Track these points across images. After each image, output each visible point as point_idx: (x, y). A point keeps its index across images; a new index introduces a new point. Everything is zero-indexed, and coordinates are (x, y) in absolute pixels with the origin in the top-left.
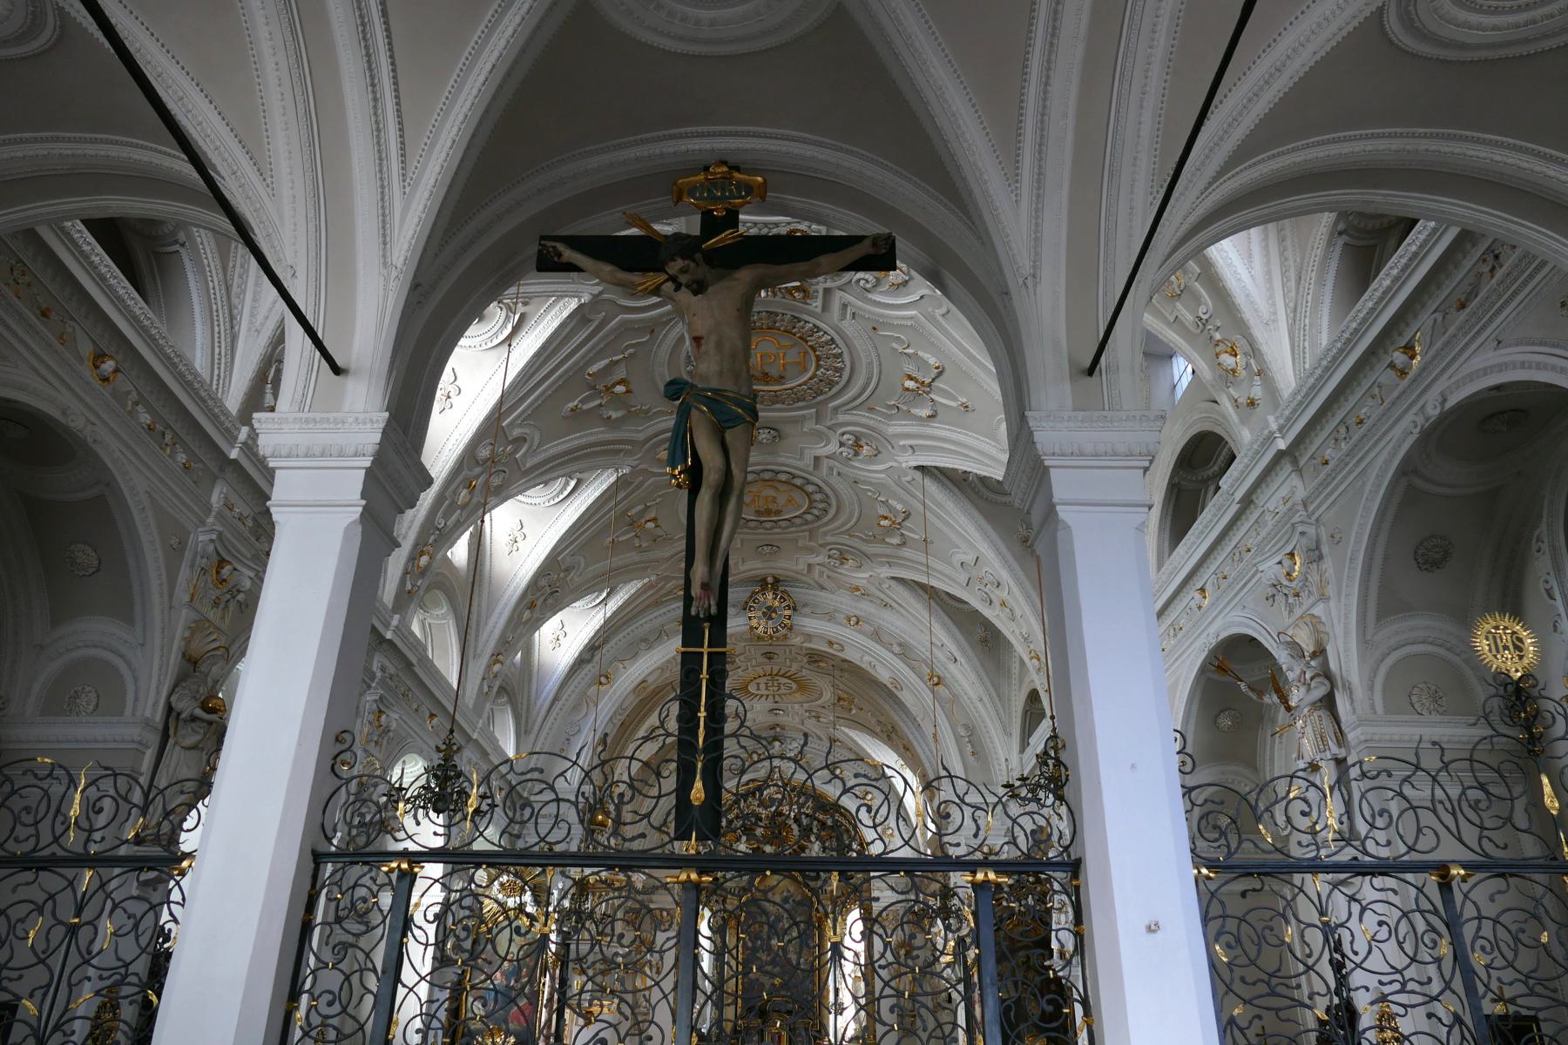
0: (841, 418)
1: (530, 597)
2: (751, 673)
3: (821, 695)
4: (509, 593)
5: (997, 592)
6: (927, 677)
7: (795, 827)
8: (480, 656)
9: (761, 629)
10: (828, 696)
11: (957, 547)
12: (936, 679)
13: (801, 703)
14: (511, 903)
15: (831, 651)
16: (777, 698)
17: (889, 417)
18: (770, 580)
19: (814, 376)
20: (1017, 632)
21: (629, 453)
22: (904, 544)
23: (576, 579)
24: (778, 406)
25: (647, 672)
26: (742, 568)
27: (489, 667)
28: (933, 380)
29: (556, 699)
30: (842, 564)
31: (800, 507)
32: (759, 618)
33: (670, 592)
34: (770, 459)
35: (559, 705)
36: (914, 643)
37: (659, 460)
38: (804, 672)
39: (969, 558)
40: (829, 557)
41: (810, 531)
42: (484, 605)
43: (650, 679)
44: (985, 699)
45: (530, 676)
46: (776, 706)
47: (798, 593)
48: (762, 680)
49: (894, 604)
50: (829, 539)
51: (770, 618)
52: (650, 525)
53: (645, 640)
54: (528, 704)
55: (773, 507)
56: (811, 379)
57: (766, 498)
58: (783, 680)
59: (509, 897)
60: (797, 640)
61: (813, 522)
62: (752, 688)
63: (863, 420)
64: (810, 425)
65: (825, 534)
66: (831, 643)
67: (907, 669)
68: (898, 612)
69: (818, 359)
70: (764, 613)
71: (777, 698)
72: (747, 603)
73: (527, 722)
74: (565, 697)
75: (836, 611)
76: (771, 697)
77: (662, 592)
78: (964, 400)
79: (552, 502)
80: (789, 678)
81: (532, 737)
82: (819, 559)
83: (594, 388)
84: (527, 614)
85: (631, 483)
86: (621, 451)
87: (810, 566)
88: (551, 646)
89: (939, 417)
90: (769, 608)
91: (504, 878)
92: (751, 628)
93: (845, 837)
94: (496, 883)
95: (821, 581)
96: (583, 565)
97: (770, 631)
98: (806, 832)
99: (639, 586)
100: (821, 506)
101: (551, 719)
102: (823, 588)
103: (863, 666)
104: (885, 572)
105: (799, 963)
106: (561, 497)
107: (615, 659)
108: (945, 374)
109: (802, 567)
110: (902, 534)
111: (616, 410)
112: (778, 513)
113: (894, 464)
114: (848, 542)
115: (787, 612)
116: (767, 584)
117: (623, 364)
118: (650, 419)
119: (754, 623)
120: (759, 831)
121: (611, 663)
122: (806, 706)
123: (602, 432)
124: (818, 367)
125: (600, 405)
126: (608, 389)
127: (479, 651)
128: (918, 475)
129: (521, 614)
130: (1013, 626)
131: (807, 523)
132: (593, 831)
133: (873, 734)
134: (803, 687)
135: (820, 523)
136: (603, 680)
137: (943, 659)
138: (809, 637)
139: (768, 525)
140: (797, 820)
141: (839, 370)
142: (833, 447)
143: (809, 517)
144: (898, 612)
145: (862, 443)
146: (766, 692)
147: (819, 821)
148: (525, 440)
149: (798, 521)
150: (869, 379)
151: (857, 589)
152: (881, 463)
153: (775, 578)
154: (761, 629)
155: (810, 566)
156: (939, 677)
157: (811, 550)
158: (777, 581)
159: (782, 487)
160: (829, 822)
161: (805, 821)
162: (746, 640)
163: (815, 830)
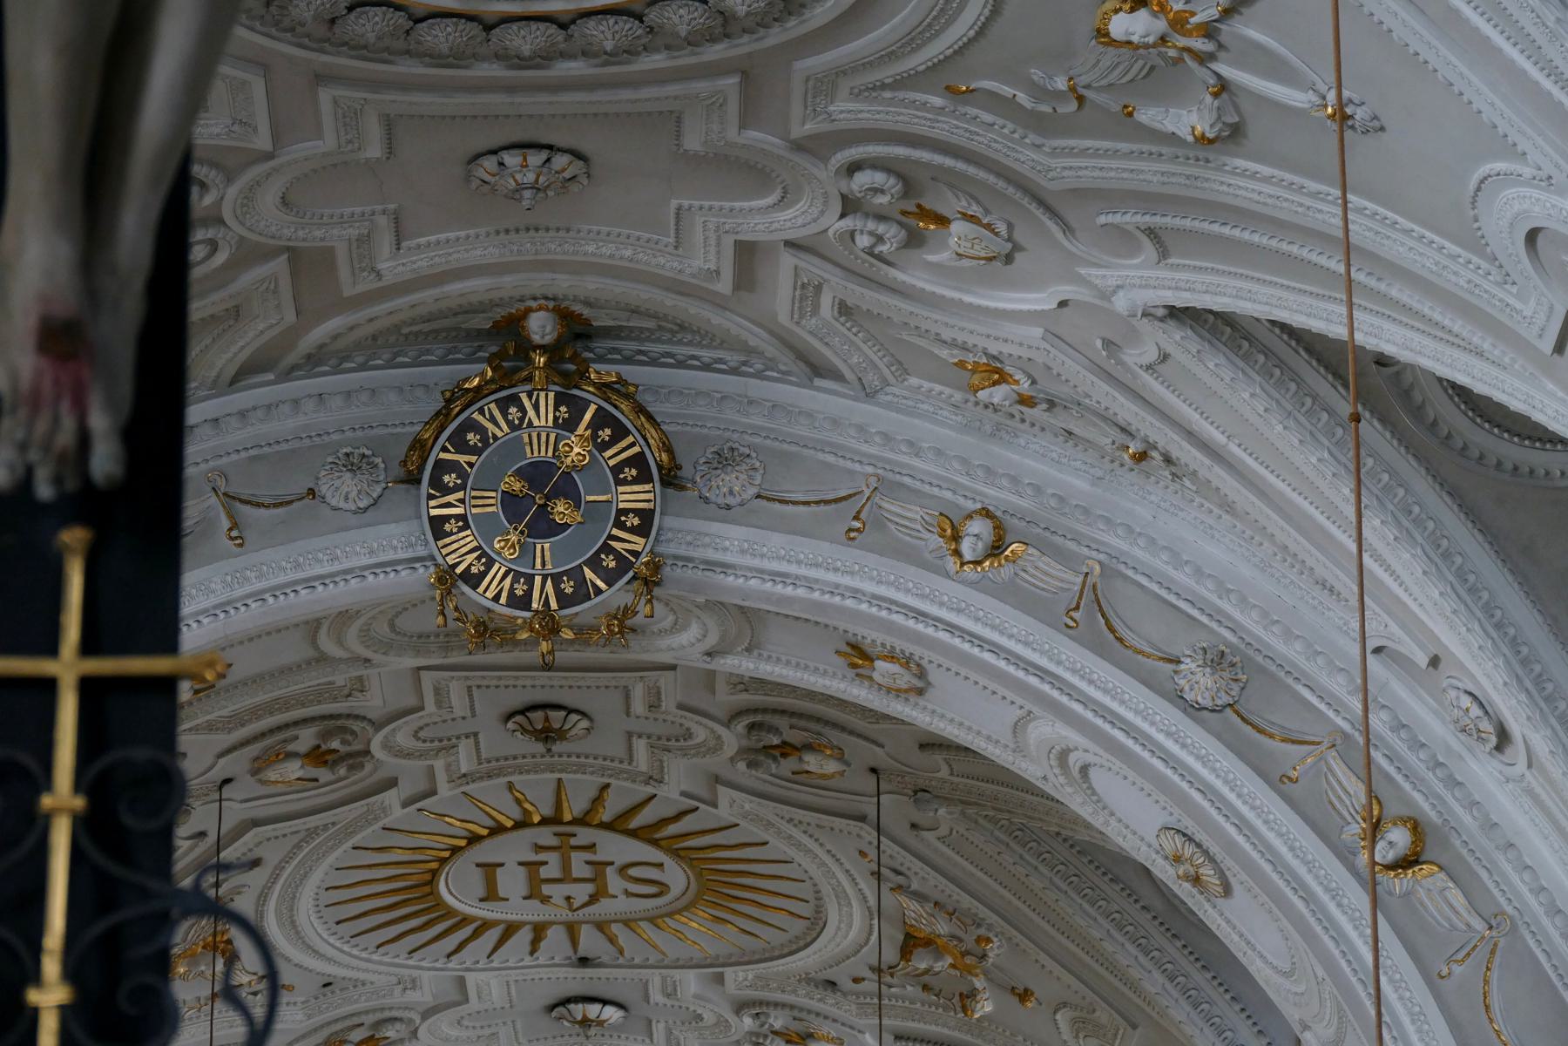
3: (816, 924)
6: (1356, 828)
9: (495, 582)
11: (1512, 152)
12: (1397, 839)
13: (714, 968)
15: (859, 693)
16: (590, 941)
18: (541, 327)
22: (1232, 135)
26: (391, 267)
30: (914, 240)
32: (488, 527)
36: (1293, 652)
38: (730, 805)
40: (849, 206)
41: (747, 74)
48: (512, 851)
50: (846, 110)
51: (544, 526)
65: (825, 85)
66: (859, 655)
67: (1252, 784)
68: (1206, 489)
70: (509, 500)
72: (420, 447)
75: (883, 486)
76: (556, 938)
80: (645, 834)
82: (795, 219)
87: (747, 253)
90: (537, 474)
92: (447, 578)
95: (804, 334)
97: (543, 593)
102: (817, 369)
103: (1031, 770)
110: (1223, 87)
114: (943, 129)
115: (633, 496)
116: (525, 348)
119: (460, 549)
122: (737, 978)
137: (1437, 729)
144: (1206, 489)
146: (533, 912)
151: (996, 373)
153: (564, 316)
154: (495, 582)
155: (747, 253)
156: (1416, 827)
162: (420, 642)
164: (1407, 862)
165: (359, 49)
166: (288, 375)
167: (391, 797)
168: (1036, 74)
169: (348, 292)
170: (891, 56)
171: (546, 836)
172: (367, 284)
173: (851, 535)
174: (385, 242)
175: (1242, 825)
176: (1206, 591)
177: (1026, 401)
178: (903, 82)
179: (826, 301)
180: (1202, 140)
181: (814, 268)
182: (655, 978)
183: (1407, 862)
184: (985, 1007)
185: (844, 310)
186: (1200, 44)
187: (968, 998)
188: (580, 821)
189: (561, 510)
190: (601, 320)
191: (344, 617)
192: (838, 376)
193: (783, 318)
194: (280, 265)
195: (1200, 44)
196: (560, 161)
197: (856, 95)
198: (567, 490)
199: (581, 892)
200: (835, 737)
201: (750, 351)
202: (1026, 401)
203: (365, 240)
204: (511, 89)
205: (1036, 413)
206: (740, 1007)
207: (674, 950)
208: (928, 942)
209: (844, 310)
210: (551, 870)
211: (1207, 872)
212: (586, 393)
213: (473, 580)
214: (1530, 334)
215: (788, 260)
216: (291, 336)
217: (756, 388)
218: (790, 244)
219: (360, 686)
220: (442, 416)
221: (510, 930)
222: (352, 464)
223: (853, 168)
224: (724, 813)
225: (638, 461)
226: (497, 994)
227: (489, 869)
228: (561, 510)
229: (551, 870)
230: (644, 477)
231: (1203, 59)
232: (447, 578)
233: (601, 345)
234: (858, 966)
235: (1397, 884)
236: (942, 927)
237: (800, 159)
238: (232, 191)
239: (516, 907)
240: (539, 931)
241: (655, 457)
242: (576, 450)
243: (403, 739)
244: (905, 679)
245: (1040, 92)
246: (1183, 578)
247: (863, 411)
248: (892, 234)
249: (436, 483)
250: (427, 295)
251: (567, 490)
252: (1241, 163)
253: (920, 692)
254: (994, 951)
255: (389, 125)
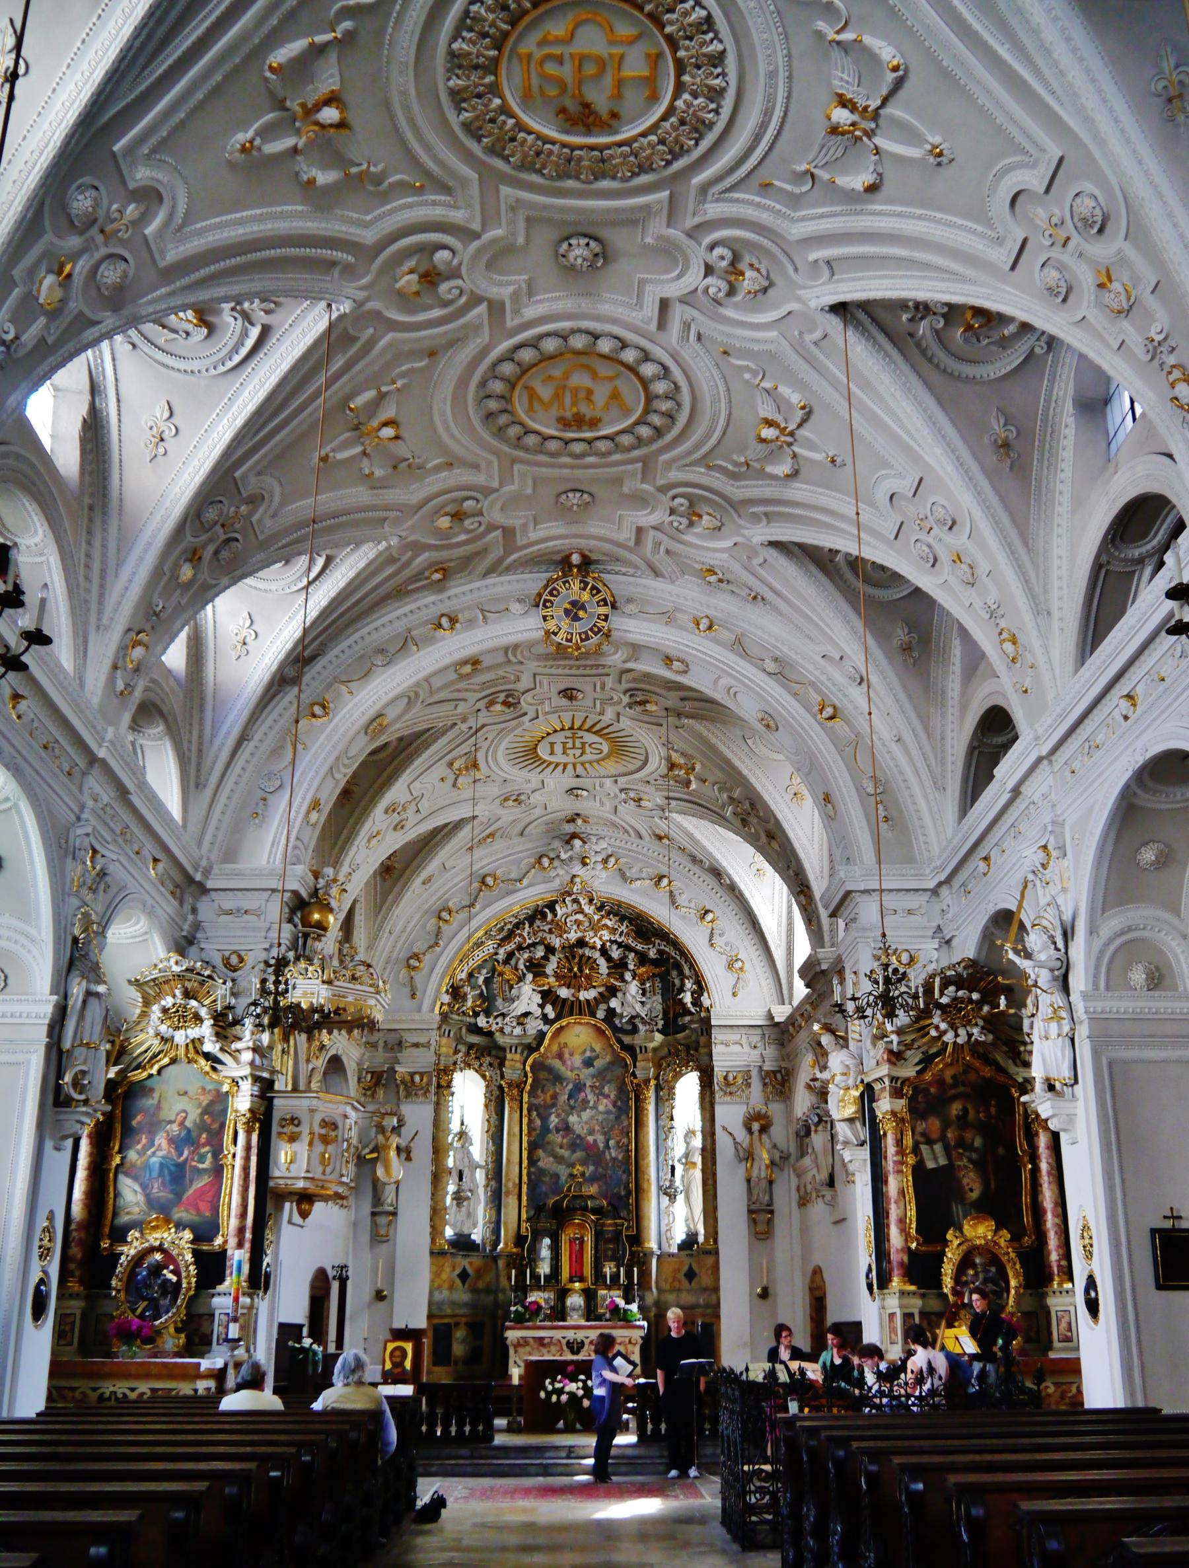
0: (714, 210)
1: (189, 539)
2: (541, 727)
3: (645, 763)
4: (152, 525)
5: (950, 539)
6: (816, 709)
7: (602, 962)
8: (107, 628)
10: (656, 764)
11: (888, 465)
12: (829, 711)
13: (615, 778)
14: (180, 1037)
17: (795, 201)
18: (576, 559)
19: (671, 111)
20: (978, 605)
21: (349, 271)
22: (795, 474)
23: (268, 523)
24: (605, 184)
25: (385, 699)
26: (533, 535)
27: (123, 650)
28: (885, 101)
29: (243, 739)
30: (691, 524)
31: (626, 411)
32: (560, 618)
33: (418, 576)
34: (585, 305)
35: (248, 747)
36: (798, 658)
37: (400, 294)
39: (905, 486)
40: (672, 512)
41: (646, 462)
42: (112, 545)
43: (392, 713)
44: (907, 736)
45: (202, 699)
46: (575, 782)
47: (618, 583)
48: (559, 738)
49: (769, 595)
50: (675, 475)
51: (576, 618)
52: (388, 432)
53: (381, 651)
54: (200, 744)
55: (586, 410)
56: (664, 118)
57: (575, 391)
58: (590, 738)
59: (177, 1028)
60: (616, 659)
61: (651, 441)
62: (543, 752)
63: (750, 213)
64: (658, 228)
65: (669, 465)
66: (668, 660)
68: (775, 608)
69: (680, 67)
70: (567, 612)
71: (579, 767)
72: (540, 595)
73: (198, 771)
74: (258, 736)
76: (570, 767)
77: (407, 573)
78: (937, 140)
79: (222, 369)
81: (209, 792)
83: (280, 105)
84: (187, 572)
85: (354, 339)
86: (333, 264)
87: (639, 531)
88: (234, 655)
89: (886, 190)
90: (574, 603)
91: (168, 1001)
92: (548, 633)
93: (674, 973)
94: (155, 1008)
96: (277, 499)
98: (618, 967)
99: (372, 555)
100: (665, 406)
101: (236, 769)
102: (657, 574)
103: (717, 696)
104: (760, 533)
105: (607, 1147)
106: (237, 359)
107: (336, 680)
108: (908, 85)
109: (626, 535)
110: (795, 456)
111: (324, 167)
112: (594, 423)
113: (793, 306)
115: (603, 610)
116: (571, 566)
117: (332, 56)
118: (385, 197)
119: (551, 625)
120: (551, 967)
121: (330, 685)
123: (300, 216)
124: (680, 88)
125: (295, 150)
126: (310, 111)
127: (105, 621)
128: (834, 323)
129: (176, 567)
130: (971, 595)
131: (640, 442)
132: (306, 936)
133: (718, 818)
134: (619, 747)
135: (660, 443)
136: (317, 710)
138: (636, 649)
139: (578, 448)
140: (604, 952)
141: (715, 94)
142: (694, 278)
143: (644, 431)
144: (775, 608)
145: (742, 266)
147: (637, 952)
148: (160, 198)
149: (626, 440)
150: (768, 113)
151: (712, 571)
152: (775, 306)
155: (639, 531)
156: (835, 707)
157: (640, 500)
158: (587, 563)
159: (605, 370)
160: (652, 954)
161: (616, 954)
162: (539, 657)
163: (631, 967)
164: (831, 718)
165: (526, 449)
166: (500, 575)
167: (526, 719)
168: (735, 457)
169: (519, 543)
170: (689, 453)
171: (569, 733)
172: (525, 542)
173: (667, 623)
174: (531, 525)
175: (783, 707)
176: (772, 640)
177: (721, 581)
178: (691, 464)
179: (662, 549)
180: (787, 476)
181: (659, 535)
182: (597, 781)
183: (831, 718)
184: (693, 786)
185: (668, 552)
186: (789, 439)
187: (688, 783)
188: (580, 729)
189: (581, 614)
190: (594, 557)
191: (516, 646)
192: (663, 576)
193: (649, 554)
194: (498, 533)
195: (789, 439)
196: (585, 496)
197: (678, 469)
198: (583, 607)
199: (578, 752)
200: (654, 698)
201: (636, 567)
202: (721, 581)
203: (525, 525)
204: (572, 467)
205: (724, 585)
206: (621, 790)
207: (603, 772)
208: (680, 767)
209: (668, 552)
210: (570, 745)
211: (772, 723)
212: (589, 580)
213: (555, 634)
214: (886, 533)
215: (652, 533)
216: (500, 561)
217: (639, 581)
218: (654, 528)
219: (518, 679)
220: (546, 586)
221: (557, 765)
222: (519, 601)
223: (674, 498)
224: (621, 725)
225: (604, 600)
226: (552, 787)
227: (552, 744)
228: (581, 614)
229: (570, 745)
230: (606, 604)
231: (790, 445)
232: (548, 633)
233: (593, 567)
234: (656, 776)
235: (830, 724)
236: (682, 761)
237: (660, 495)
238: (486, 503)
239: (559, 758)
240: (565, 766)
241: (609, 599)
242: (586, 596)
243: (529, 699)
244: (681, 667)
245: (736, 464)
246: (766, 637)
247: (670, 587)
248: (685, 521)
249: (545, 606)
250: (543, 546)
251: (583, 607)
252: (797, 485)
253: (686, 672)
254: (698, 767)
255: (535, 482)
